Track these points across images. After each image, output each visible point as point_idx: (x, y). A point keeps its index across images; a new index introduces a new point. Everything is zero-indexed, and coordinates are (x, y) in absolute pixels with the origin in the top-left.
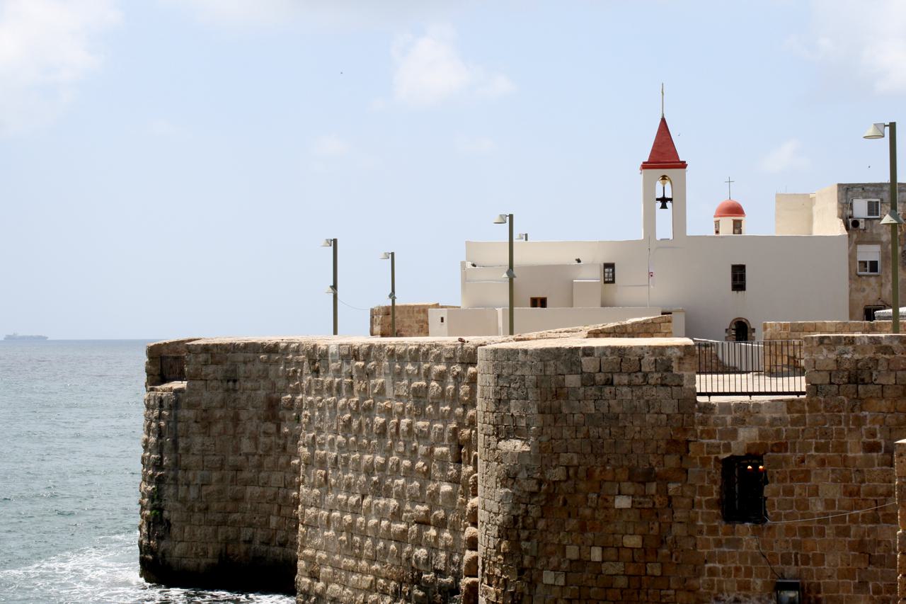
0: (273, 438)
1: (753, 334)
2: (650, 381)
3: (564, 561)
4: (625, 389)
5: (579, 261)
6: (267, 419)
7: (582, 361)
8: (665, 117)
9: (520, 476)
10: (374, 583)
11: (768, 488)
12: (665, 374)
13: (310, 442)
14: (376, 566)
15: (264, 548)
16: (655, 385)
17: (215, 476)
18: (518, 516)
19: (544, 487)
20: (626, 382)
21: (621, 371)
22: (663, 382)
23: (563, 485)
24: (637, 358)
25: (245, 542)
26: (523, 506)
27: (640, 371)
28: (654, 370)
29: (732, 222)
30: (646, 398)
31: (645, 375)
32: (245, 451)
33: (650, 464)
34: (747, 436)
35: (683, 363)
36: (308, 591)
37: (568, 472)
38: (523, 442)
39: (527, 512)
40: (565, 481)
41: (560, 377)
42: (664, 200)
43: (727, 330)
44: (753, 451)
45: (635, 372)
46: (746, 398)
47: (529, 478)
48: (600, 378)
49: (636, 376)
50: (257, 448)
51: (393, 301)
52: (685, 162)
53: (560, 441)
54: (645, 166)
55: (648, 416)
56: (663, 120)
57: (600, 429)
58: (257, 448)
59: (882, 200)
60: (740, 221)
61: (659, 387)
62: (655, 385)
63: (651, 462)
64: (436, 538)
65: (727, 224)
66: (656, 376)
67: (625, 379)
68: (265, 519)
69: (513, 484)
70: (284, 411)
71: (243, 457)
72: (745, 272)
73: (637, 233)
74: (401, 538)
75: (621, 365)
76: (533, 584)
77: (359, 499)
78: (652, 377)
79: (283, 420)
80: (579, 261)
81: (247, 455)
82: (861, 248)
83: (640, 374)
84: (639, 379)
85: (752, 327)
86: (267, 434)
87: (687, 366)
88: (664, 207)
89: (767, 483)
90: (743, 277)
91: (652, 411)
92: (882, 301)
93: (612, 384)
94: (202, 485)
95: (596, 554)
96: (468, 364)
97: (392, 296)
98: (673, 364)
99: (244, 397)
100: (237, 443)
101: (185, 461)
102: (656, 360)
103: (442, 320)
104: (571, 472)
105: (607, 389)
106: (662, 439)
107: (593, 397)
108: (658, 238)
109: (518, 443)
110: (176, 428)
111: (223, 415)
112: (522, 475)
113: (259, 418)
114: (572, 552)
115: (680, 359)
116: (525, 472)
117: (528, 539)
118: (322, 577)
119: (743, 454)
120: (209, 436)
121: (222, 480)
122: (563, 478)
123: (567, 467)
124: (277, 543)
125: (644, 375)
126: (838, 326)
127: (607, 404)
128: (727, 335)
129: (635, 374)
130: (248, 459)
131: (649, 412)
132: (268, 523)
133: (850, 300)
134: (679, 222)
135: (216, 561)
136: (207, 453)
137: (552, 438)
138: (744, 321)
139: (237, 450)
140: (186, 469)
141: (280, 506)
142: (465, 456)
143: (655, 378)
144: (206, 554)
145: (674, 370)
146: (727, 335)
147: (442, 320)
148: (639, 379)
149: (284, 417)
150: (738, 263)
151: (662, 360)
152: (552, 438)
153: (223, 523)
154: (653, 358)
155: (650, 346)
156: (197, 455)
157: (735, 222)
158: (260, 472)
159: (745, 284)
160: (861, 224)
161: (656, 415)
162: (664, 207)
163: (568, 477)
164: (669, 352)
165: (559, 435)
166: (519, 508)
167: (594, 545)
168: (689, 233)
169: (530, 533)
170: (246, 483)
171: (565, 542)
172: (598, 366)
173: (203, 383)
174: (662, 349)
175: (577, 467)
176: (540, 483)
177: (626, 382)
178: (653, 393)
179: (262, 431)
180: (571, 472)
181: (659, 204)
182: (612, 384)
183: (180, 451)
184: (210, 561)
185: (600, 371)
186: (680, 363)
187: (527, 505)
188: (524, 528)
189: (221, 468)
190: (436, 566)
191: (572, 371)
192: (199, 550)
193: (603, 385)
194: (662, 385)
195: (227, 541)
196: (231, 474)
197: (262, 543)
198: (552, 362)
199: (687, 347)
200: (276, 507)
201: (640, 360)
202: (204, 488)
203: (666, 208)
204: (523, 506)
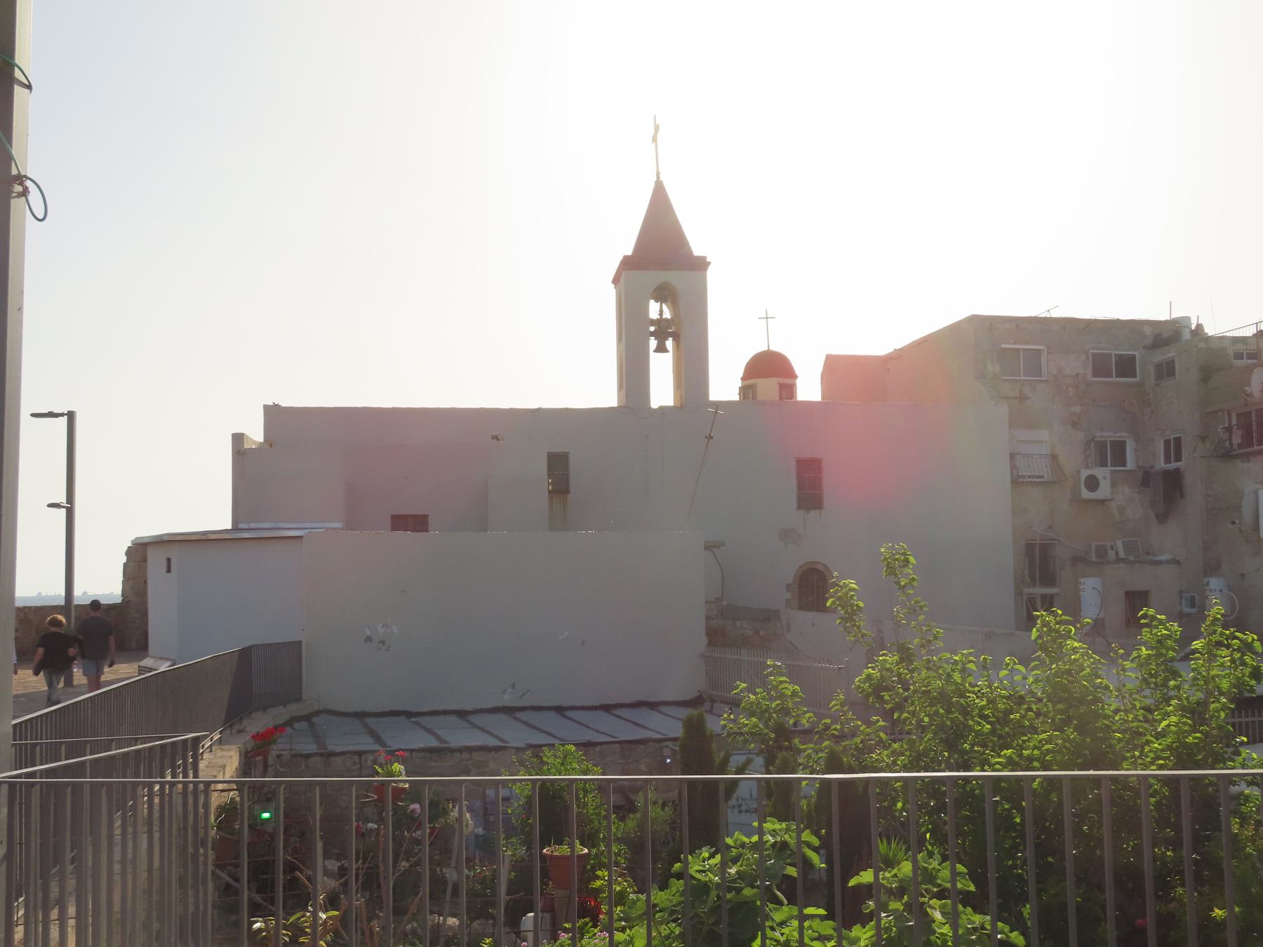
8: (662, 178)
29: (778, 386)
43: (788, 586)
52: (704, 258)
54: (628, 264)
65: (768, 387)
108: (655, 404)
128: (788, 596)
138: (820, 568)
146: (788, 596)
157: (782, 386)
162: (661, 349)
181: (653, 343)
203: (666, 351)
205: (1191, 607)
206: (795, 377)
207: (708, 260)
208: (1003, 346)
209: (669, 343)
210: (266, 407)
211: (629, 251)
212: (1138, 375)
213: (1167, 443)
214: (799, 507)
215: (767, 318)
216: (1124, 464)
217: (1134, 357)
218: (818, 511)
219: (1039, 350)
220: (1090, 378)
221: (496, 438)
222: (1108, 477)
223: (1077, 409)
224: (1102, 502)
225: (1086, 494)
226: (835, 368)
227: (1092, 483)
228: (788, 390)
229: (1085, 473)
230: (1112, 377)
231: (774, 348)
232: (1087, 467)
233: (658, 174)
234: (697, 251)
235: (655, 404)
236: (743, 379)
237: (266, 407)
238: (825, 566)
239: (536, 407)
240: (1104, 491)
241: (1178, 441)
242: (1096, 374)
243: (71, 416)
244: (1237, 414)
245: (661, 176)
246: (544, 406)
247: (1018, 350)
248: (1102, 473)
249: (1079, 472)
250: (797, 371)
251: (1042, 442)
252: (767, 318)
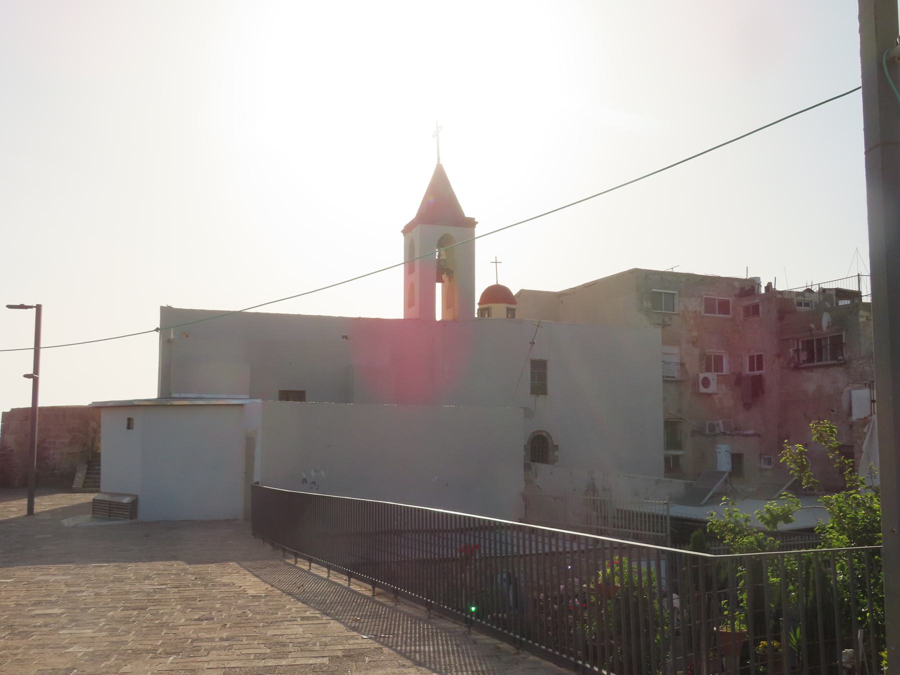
1: (556, 453)
52: (474, 219)
85: (555, 444)
138: (544, 434)
157: (508, 309)
205: (768, 465)
207: (476, 220)
208: (653, 290)
210: (162, 308)
212: (731, 313)
213: (751, 358)
214: (532, 393)
215: (496, 262)
216: (722, 371)
217: (728, 301)
218: (544, 396)
220: (703, 313)
221: (345, 337)
222: (715, 378)
223: (695, 334)
225: (702, 390)
227: (706, 383)
229: (702, 376)
231: (499, 283)
232: (702, 372)
233: (439, 159)
234: (468, 213)
237: (162, 308)
238: (548, 434)
239: (358, 316)
240: (712, 389)
241: (760, 358)
243: (39, 308)
244: (802, 341)
245: (441, 160)
246: (362, 316)
247: (661, 293)
248: (712, 376)
249: (698, 375)
251: (674, 354)
252: (496, 262)
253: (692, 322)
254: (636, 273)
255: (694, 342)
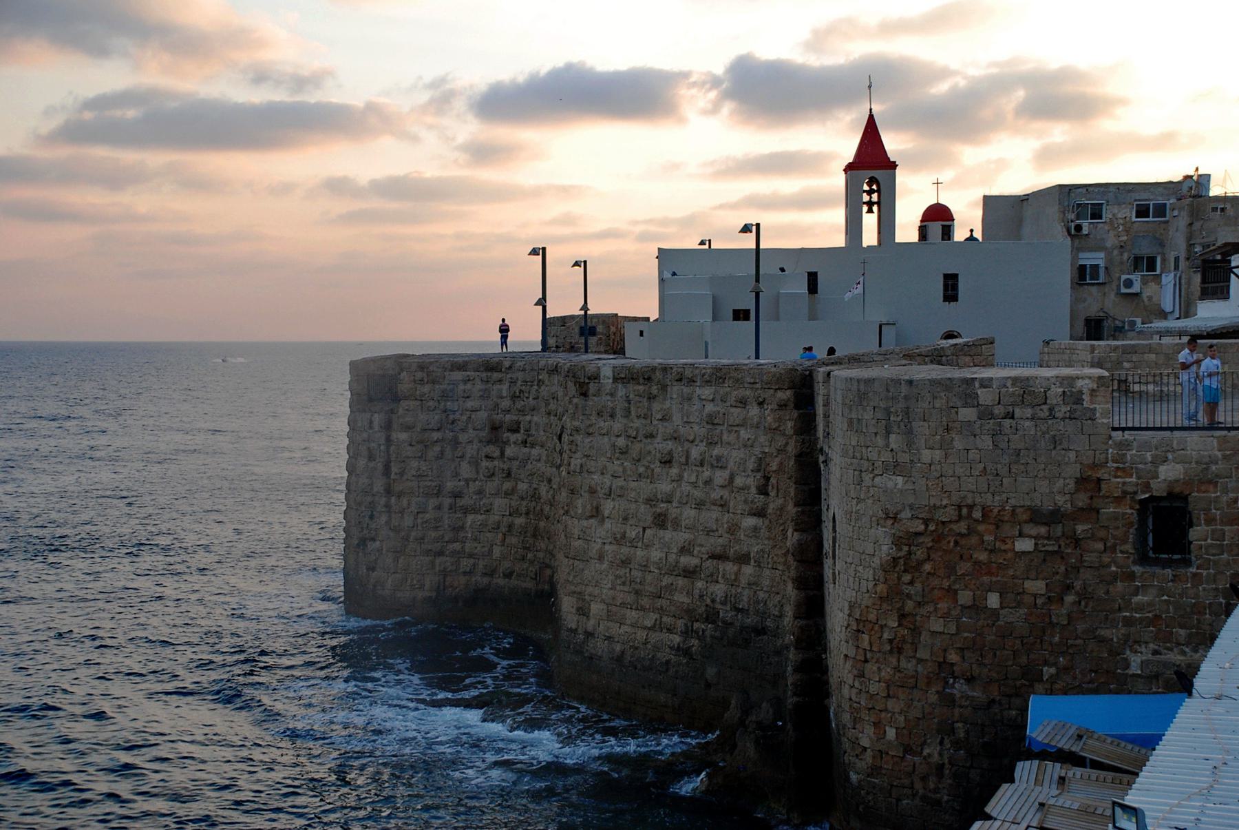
0: (496, 463)
2: (1057, 415)
3: (954, 607)
4: (1027, 424)
5: (782, 270)
6: (489, 442)
7: (979, 393)
9: (902, 515)
10: (658, 622)
11: (1194, 531)
12: (1074, 407)
13: (578, 471)
14: (659, 603)
15: (486, 580)
16: (1063, 419)
17: (432, 502)
18: (900, 558)
19: (932, 527)
20: (1029, 416)
21: (1023, 402)
22: (1072, 416)
23: (954, 527)
24: (1042, 390)
25: (465, 573)
26: (906, 548)
27: (1045, 403)
28: (1061, 402)
30: (1052, 433)
31: (1051, 410)
32: (466, 476)
33: (1055, 504)
34: (1169, 472)
35: (1096, 396)
36: (576, 630)
37: (960, 511)
38: (906, 479)
39: (910, 553)
40: (957, 522)
41: (953, 411)
42: (870, 204)
44: (1177, 490)
45: (1040, 405)
46: (1168, 433)
47: (913, 517)
48: (998, 410)
49: (1041, 410)
50: (478, 473)
51: (586, 312)
52: (895, 162)
53: (952, 479)
55: (1054, 452)
56: (871, 117)
57: (999, 466)
58: (478, 473)
59: (1108, 202)
60: (949, 226)
61: (1067, 420)
62: (1063, 419)
63: (1057, 502)
64: (737, 574)
65: (935, 228)
66: (1065, 409)
67: (1028, 412)
68: (486, 549)
69: (893, 524)
70: (509, 434)
71: (462, 483)
72: (957, 281)
73: (839, 241)
74: (689, 573)
75: (1023, 397)
76: (916, 631)
77: (639, 532)
78: (1060, 411)
79: (507, 442)
80: (782, 270)
81: (467, 481)
82: (1081, 255)
83: (1045, 407)
84: (1044, 412)
86: (490, 458)
87: (1099, 399)
88: (870, 211)
89: (1191, 525)
90: (955, 287)
91: (1058, 448)
92: (1104, 312)
93: (1013, 417)
94: (418, 513)
95: (993, 600)
96: (776, 389)
97: (585, 307)
98: (1084, 397)
99: (464, 418)
100: (455, 468)
101: (398, 488)
102: (1064, 392)
103: (641, 333)
104: (965, 511)
105: (1008, 421)
106: (1070, 478)
107: (991, 432)
108: (865, 245)
109: (900, 480)
110: (388, 452)
111: (440, 438)
112: (906, 514)
113: (481, 441)
114: (965, 597)
115: (1093, 390)
116: (908, 511)
117: (911, 583)
118: (594, 615)
119: (1165, 494)
120: (425, 460)
121: (439, 507)
122: (955, 518)
123: (960, 507)
124: (501, 575)
125: (1050, 409)
126: (1176, 348)
127: (1007, 440)
129: (1039, 408)
130: (468, 484)
131: (1055, 448)
132: (490, 551)
133: (1071, 311)
134: (886, 225)
135: (434, 594)
136: (424, 478)
137: (942, 476)
139: (456, 475)
140: (400, 495)
141: (504, 535)
142: (773, 488)
143: (1063, 410)
144: (422, 587)
145: (1085, 403)
147: (641, 333)
148: (1044, 412)
149: (509, 441)
150: (949, 272)
151: (1070, 391)
152: (942, 476)
153: (440, 553)
154: (1061, 390)
155: (1057, 377)
156: (411, 481)
157: (943, 226)
158: (481, 499)
159: (957, 294)
160: (1084, 228)
161: (1064, 451)
162: (870, 211)
163: (960, 516)
164: (1080, 383)
165: (951, 472)
166: (901, 550)
167: (990, 591)
168: (896, 241)
169: (913, 577)
170: (466, 511)
171: (957, 586)
172: (997, 399)
173: (418, 403)
174: (1072, 379)
175: (971, 507)
176: (926, 522)
177: (1029, 416)
178: (1060, 428)
179: (483, 455)
180: (965, 511)
181: (865, 208)
182: (1013, 417)
183: (393, 476)
184: (428, 594)
185: (999, 403)
186: (1091, 395)
187: (910, 546)
188: (905, 571)
189: (438, 495)
190: (737, 605)
191: (966, 403)
192: (415, 582)
193: (1002, 418)
194: (1070, 418)
195: (444, 573)
196: (447, 501)
197: (485, 574)
198: (943, 394)
199: (1100, 378)
200: (500, 536)
201: (1045, 392)
202: (420, 516)
204: (906, 548)
206: (953, 220)
209: (875, 208)
211: (851, 161)
216: (1155, 270)
219: (1102, 204)
220: (1134, 219)
223: (1125, 238)
224: (1136, 294)
225: (1124, 290)
226: (990, 202)
227: (1129, 283)
228: (947, 233)
229: (1124, 277)
230: (1149, 217)
233: (871, 110)
235: (865, 245)
236: (922, 221)
237: (659, 249)
240: (1136, 288)
242: (1136, 217)
243: (585, 262)
248: (1136, 277)
250: (955, 217)
253: (1121, 228)
254: (1061, 186)
255: (1121, 246)
